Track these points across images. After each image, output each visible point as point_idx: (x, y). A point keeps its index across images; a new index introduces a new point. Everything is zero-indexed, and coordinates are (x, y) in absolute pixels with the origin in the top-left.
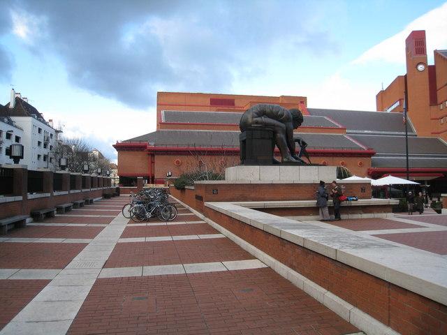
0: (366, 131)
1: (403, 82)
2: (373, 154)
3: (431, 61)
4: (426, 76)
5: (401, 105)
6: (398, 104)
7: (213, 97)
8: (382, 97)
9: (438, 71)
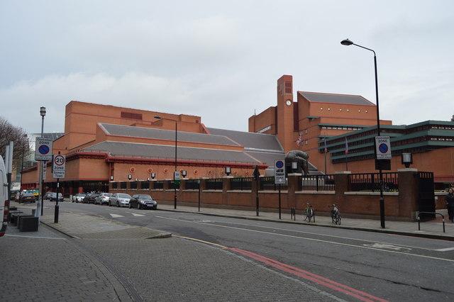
0: (250, 149)
1: (274, 111)
2: (267, 167)
3: (295, 100)
4: (292, 109)
5: (272, 129)
6: (269, 128)
7: (125, 111)
8: (254, 121)
9: (300, 107)
